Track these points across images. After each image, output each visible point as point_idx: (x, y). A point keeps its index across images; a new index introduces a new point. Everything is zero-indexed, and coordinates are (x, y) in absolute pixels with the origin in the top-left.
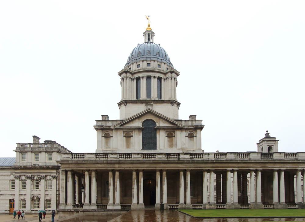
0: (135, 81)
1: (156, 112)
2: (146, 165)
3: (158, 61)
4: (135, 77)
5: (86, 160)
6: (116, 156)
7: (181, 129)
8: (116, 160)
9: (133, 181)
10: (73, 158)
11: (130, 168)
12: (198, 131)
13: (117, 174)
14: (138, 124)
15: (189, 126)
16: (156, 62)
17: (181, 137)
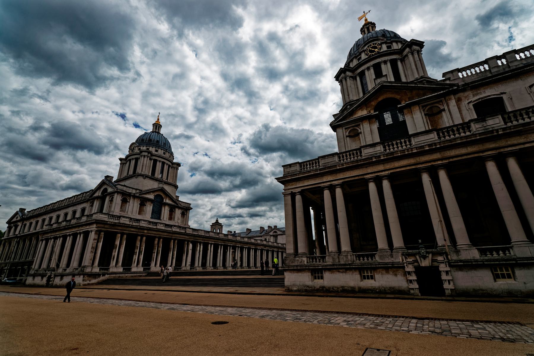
0: (152, 161)
1: (167, 191)
2: (166, 234)
3: (164, 150)
4: (154, 158)
5: (121, 223)
6: (146, 223)
7: (179, 208)
8: (144, 226)
9: (155, 246)
10: (109, 219)
11: (155, 234)
12: (188, 211)
13: (144, 238)
14: (151, 196)
15: (184, 207)
16: (169, 154)
17: (178, 213)
